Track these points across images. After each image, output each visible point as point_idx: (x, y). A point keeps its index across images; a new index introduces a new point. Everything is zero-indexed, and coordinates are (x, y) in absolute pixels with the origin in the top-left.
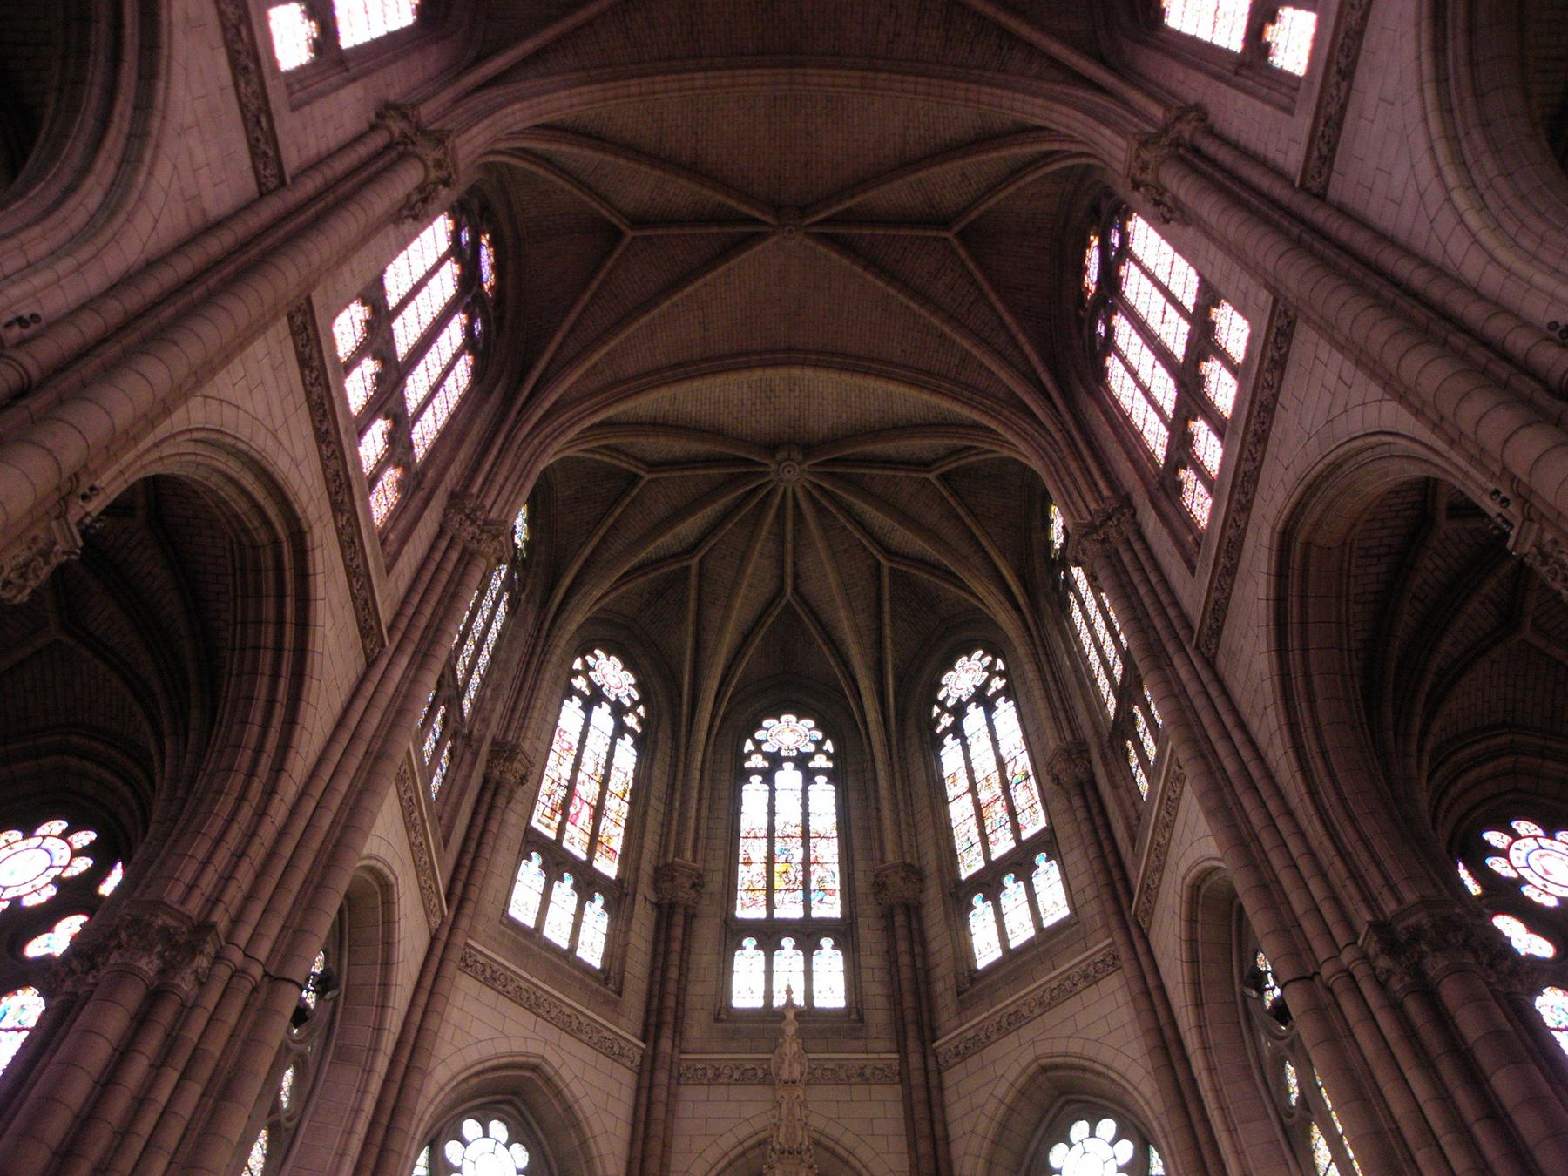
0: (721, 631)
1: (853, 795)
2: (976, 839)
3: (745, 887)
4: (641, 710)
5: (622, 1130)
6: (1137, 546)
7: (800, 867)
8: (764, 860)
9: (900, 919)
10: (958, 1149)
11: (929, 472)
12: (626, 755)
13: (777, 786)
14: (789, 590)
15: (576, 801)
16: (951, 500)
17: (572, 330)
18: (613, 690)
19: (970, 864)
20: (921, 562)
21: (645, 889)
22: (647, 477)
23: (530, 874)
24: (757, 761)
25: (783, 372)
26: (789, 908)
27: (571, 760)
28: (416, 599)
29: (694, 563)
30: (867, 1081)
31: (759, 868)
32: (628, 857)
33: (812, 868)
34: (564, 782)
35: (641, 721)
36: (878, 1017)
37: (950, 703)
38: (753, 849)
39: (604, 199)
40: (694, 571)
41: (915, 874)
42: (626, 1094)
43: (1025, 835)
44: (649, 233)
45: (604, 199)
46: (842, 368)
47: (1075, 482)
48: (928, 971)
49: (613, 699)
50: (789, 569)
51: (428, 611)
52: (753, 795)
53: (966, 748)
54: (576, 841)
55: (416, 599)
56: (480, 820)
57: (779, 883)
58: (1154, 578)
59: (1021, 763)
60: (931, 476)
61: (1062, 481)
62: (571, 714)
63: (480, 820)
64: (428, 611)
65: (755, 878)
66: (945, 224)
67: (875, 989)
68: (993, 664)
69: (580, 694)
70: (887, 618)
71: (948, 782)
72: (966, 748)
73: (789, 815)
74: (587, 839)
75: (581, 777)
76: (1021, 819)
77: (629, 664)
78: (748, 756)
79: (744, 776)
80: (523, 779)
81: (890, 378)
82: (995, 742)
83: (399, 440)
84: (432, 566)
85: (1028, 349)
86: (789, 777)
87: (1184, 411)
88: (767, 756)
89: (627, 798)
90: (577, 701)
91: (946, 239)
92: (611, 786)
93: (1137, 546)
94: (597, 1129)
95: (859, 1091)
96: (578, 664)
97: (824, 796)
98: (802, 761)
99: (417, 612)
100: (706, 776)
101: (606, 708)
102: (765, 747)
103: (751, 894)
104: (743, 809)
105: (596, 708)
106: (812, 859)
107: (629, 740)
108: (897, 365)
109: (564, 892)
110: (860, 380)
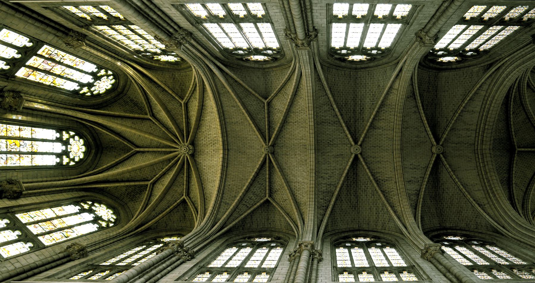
0: (122, 125)
1: (52, 172)
3: (8, 128)
4: (89, 94)
6: (178, 262)
7: (18, 150)
8: (21, 136)
11: (186, 196)
12: (71, 86)
13: (55, 143)
14: (138, 149)
15: (53, 64)
16: (176, 203)
17: (236, 81)
18: (98, 85)
20: (151, 195)
22: (182, 103)
23: (23, 41)
24: (65, 136)
25: (221, 147)
27: (71, 65)
28: (159, 13)
29: (149, 116)
31: (17, 134)
33: (18, 155)
35: (85, 93)
37: (93, 208)
39: (276, 95)
40: (146, 116)
43: (40, 238)
44: (266, 108)
45: (276, 95)
46: (223, 166)
47: (194, 241)
49: (95, 84)
50: (146, 149)
51: (155, 17)
52: (52, 134)
53: (76, 214)
54: (35, 62)
55: (159, 13)
56: (53, 25)
57: (10, 142)
58: (169, 268)
60: (184, 197)
61: (194, 237)
62: (92, 68)
63: (53, 25)
64: (155, 17)
65: (12, 132)
66: (270, 196)
68: (111, 222)
69: (98, 72)
70: (127, 184)
71: (60, 208)
72: (76, 214)
73: (40, 147)
74: (36, 66)
75: (64, 68)
76: (47, 236)
77: (108, 92)
78: (68, 133)
79: (59, 130)
80: (68, 44)
81: (221, 181)
82: (80, 224)
83: (214, 19)
84: (169, 22)
85: (234, 223)
86: (59, 148)
87: (230, 270)
88: (68, 140)
89: (52, 85)
90: (95, 70)
91: (266, 196)
93: (178, 262)
96: (110, 73)
98: (66, 153)
99: (155, 13)
100: (61, 116)
101: (92, 81)
102: (71, 140)
103: (5, 130)
105: (92, 77)
106: (22, 155)
107: (77, 88)
108: (225, 183)
109: (12, 53)
110: (220, 171)
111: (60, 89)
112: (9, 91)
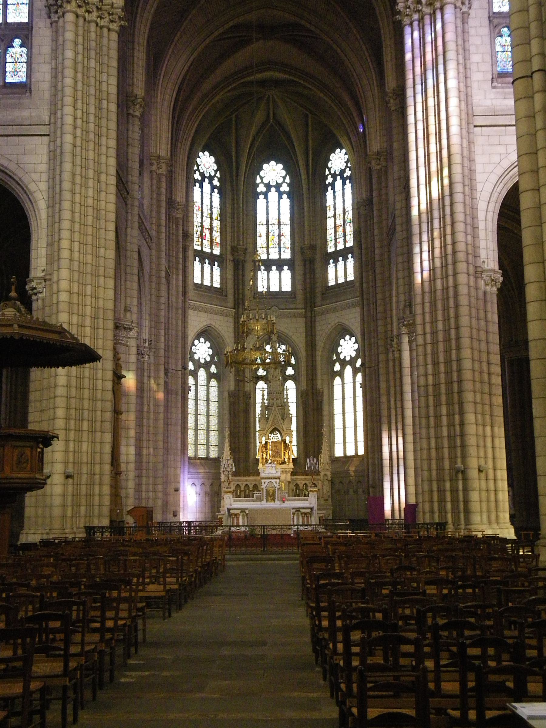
2: (333, 238)
5: (232, 335)
9: (308, 266)
10: (318, 338)
12: (216, 197)
19: (331, 249)
21: (230, 257)
23: (197, 265)
26: (274, 256)
29: (234, 116)
30: (296, 317)
31: (264, 238)
32: (222, 244)
33: (282, 238)
34: (200, 225)
35: (219, 180)
36: (300, 296)
38: (261, 230)
41: (313, 247)
42: (232, 325)
48: (315, 283)
52: (261, 202)
57: (271, 245)
59: (350, 215)
67: (299, 287)
78: (258, 186)
79: (256, 195)
86: (273, 195)
92: (214, 217)
94: (226, 337)
95: (294, 320)
97: (286, 202)
102: (266, 181)
104: (258, 211)
111: (220, 209)
112: (233, 255)
